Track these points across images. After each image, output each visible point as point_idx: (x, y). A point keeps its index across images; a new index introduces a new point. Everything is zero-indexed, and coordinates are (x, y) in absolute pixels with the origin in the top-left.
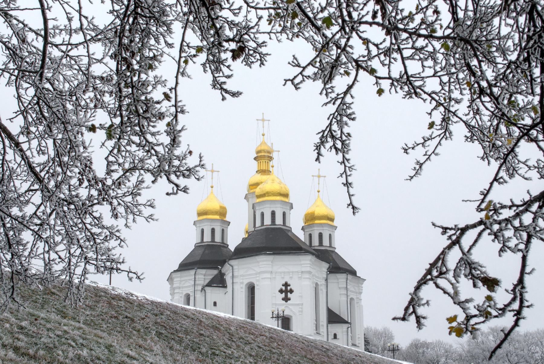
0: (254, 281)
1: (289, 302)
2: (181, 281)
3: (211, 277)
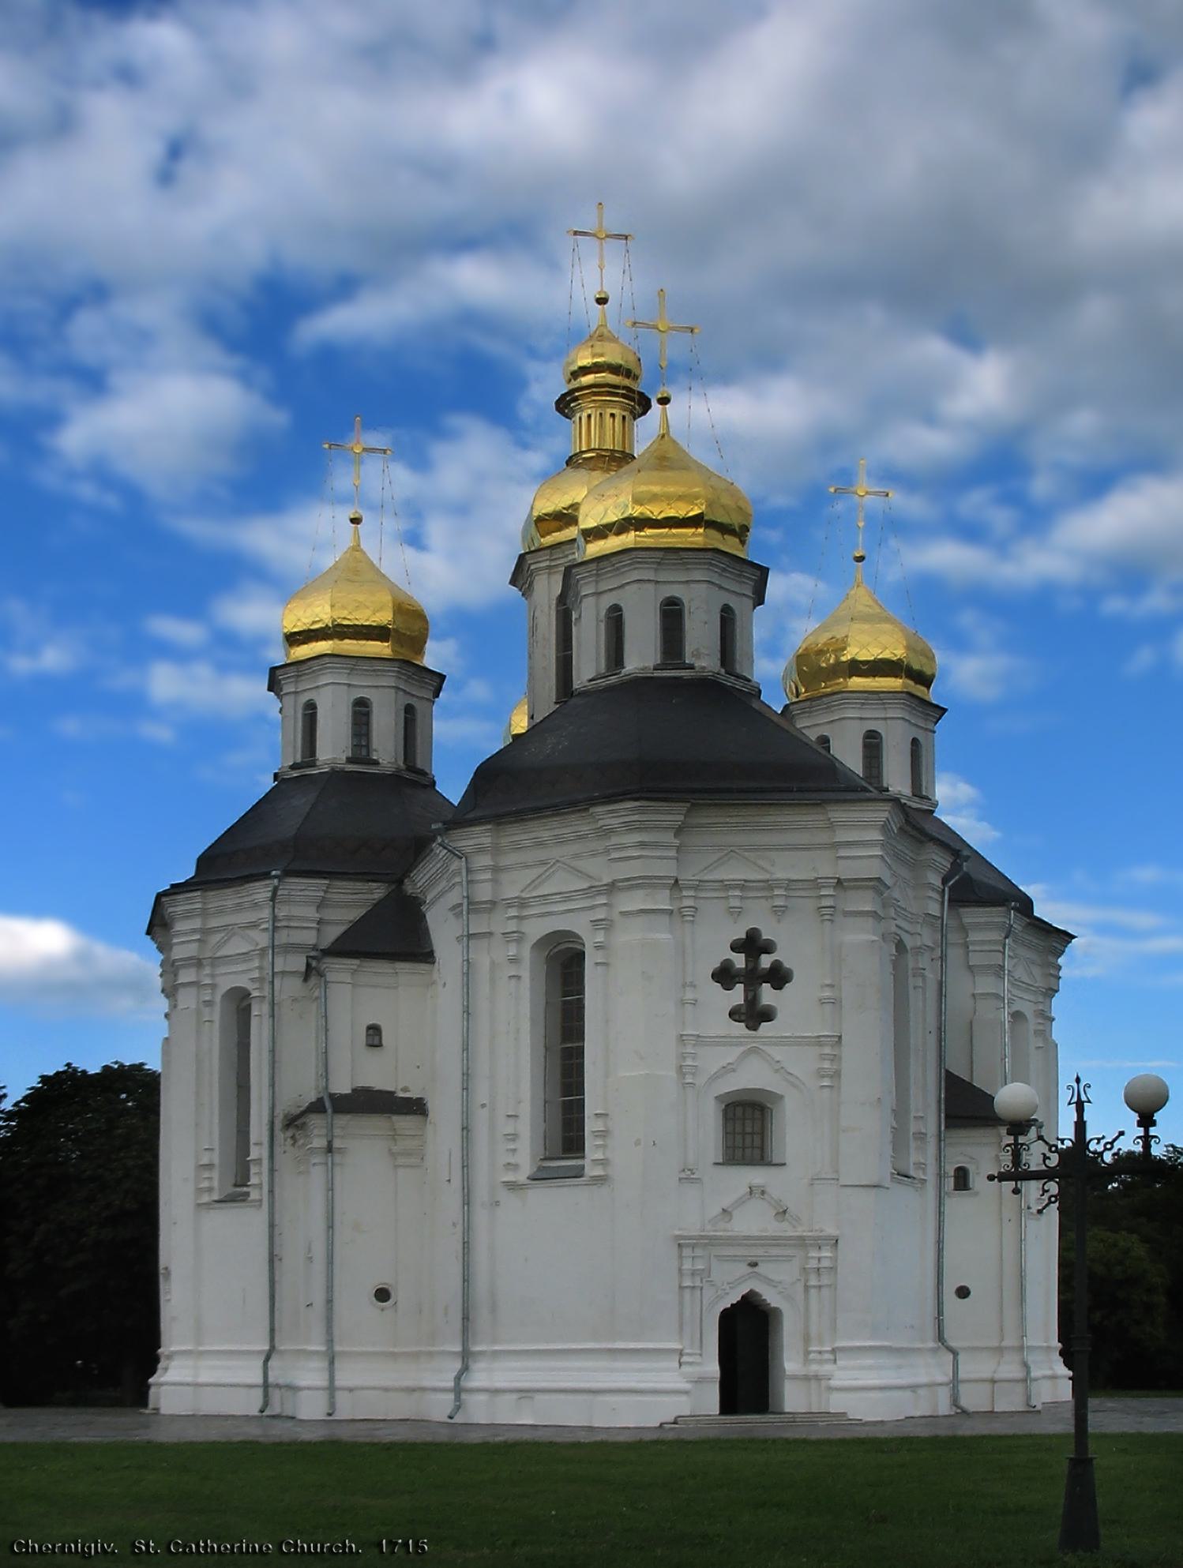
2: (206, 932)
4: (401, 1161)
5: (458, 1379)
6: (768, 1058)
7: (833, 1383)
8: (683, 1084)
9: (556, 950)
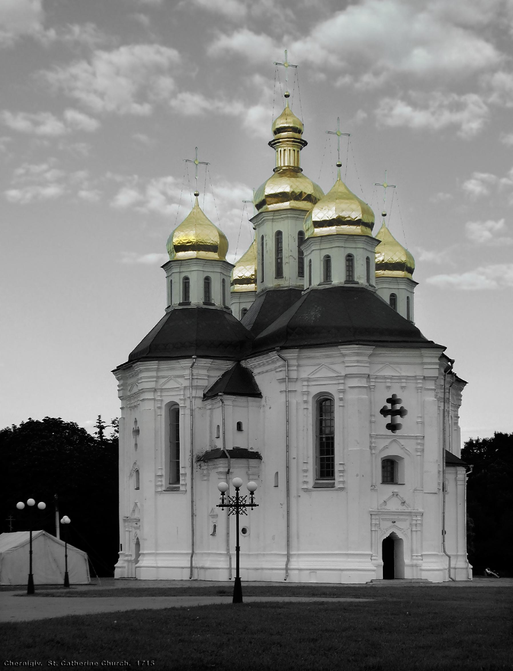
0: (332, 389)
1: (398, 432)
2: (158, 377)
3: (219, 374)
4: (251, 477)
5: (287, 565)
6: (399, 444)
7: (423, 568)
8: (371, 453)
9: (318, 399)
